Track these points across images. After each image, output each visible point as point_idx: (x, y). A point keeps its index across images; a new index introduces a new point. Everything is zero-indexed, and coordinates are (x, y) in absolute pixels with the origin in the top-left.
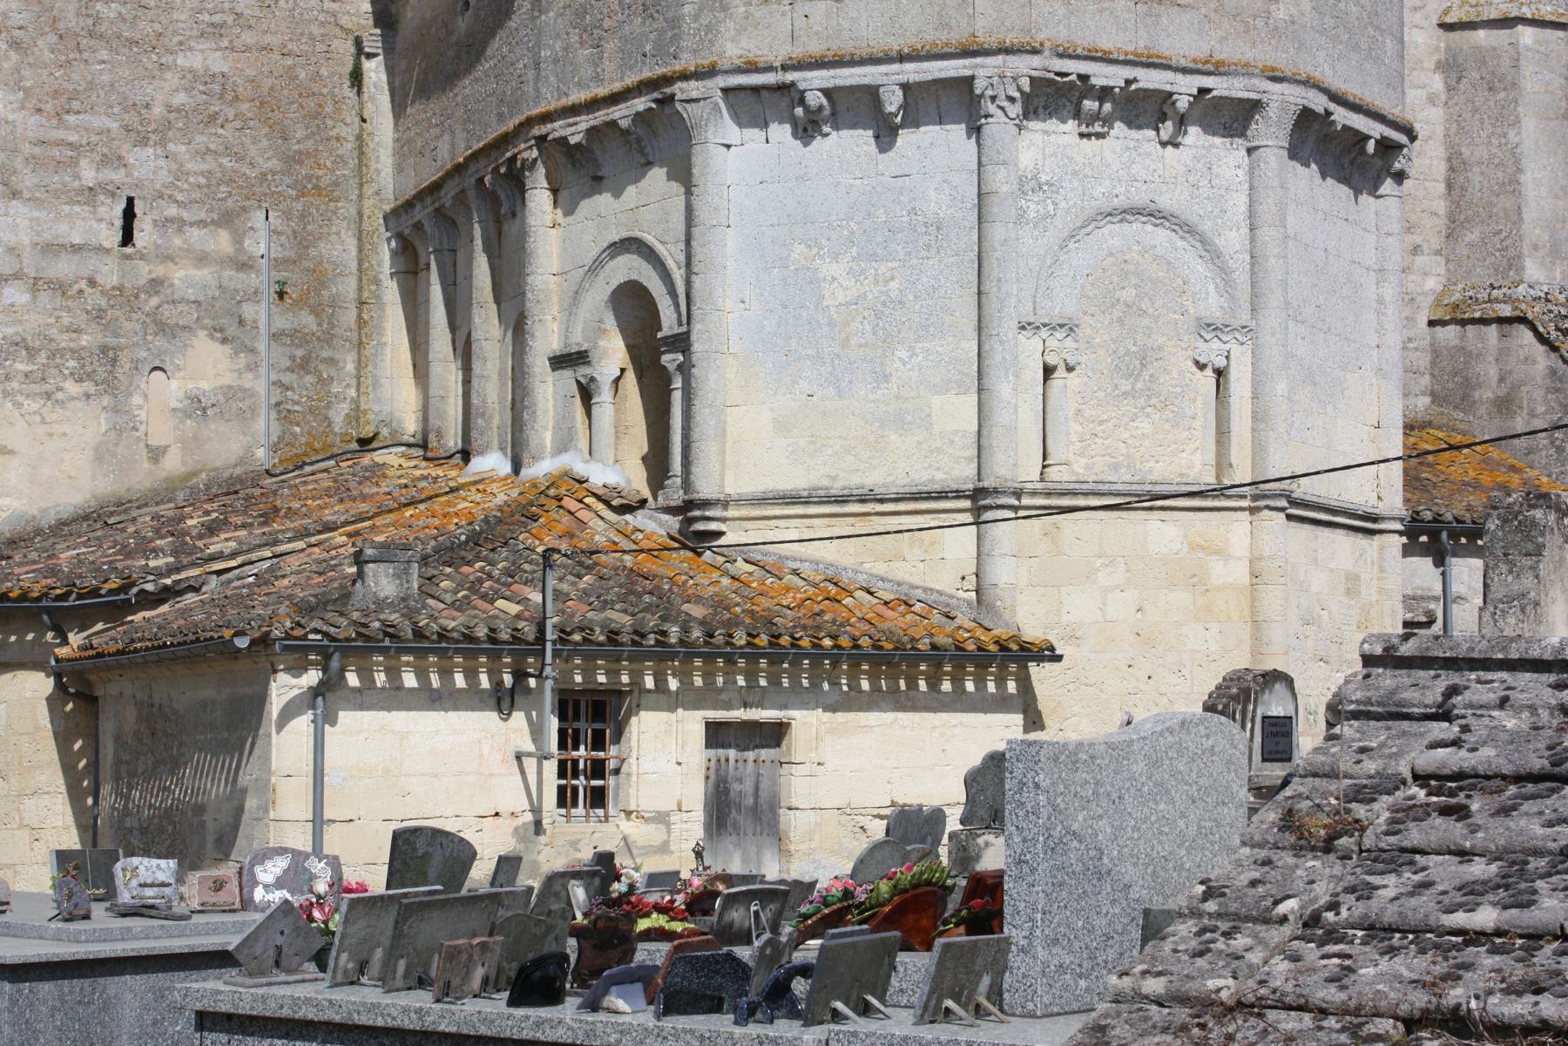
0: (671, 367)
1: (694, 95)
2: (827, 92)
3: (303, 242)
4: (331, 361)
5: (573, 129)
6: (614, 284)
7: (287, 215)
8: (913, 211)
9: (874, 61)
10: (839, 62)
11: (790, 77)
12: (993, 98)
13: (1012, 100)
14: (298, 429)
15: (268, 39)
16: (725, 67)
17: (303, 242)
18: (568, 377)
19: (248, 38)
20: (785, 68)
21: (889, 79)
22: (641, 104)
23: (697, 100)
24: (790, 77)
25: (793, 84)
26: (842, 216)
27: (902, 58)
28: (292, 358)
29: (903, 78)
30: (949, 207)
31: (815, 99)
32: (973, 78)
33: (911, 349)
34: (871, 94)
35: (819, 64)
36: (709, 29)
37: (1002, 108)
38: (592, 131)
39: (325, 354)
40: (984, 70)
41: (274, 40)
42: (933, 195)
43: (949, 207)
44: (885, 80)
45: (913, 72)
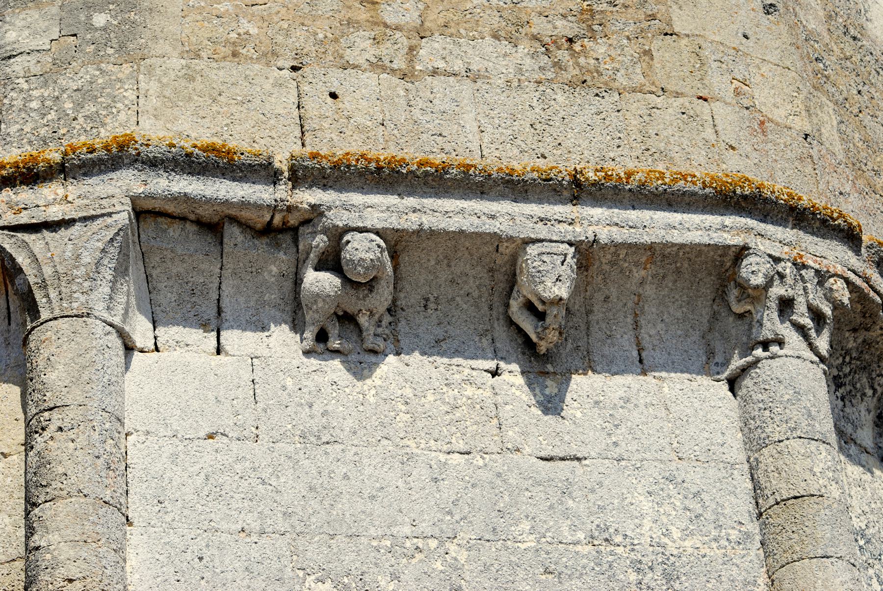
1: (55, 213)
8: (601, 537)
9: (514, 187)
10: (435, 180)
11: (307, 197)
12: (786, 305)
13: (817, 316)
16: (153, 152)
20: (300, 175)
21: (550, 240)
23: (67, 223)
24: (307, 197)
25: (317, 211)
26: (425, 527)
27: (578, 190)
29: (580, 232)
30: (687, 534)
31: (362, 249)
32: (742, 252)
34: (502, 263)
35: (385, 177)
36: (84, 95)
37: (801, 329)
40: (768, 244)
42: (646, 505)
43: (687, 534)
44: (542, 231)
45: (600, 222)
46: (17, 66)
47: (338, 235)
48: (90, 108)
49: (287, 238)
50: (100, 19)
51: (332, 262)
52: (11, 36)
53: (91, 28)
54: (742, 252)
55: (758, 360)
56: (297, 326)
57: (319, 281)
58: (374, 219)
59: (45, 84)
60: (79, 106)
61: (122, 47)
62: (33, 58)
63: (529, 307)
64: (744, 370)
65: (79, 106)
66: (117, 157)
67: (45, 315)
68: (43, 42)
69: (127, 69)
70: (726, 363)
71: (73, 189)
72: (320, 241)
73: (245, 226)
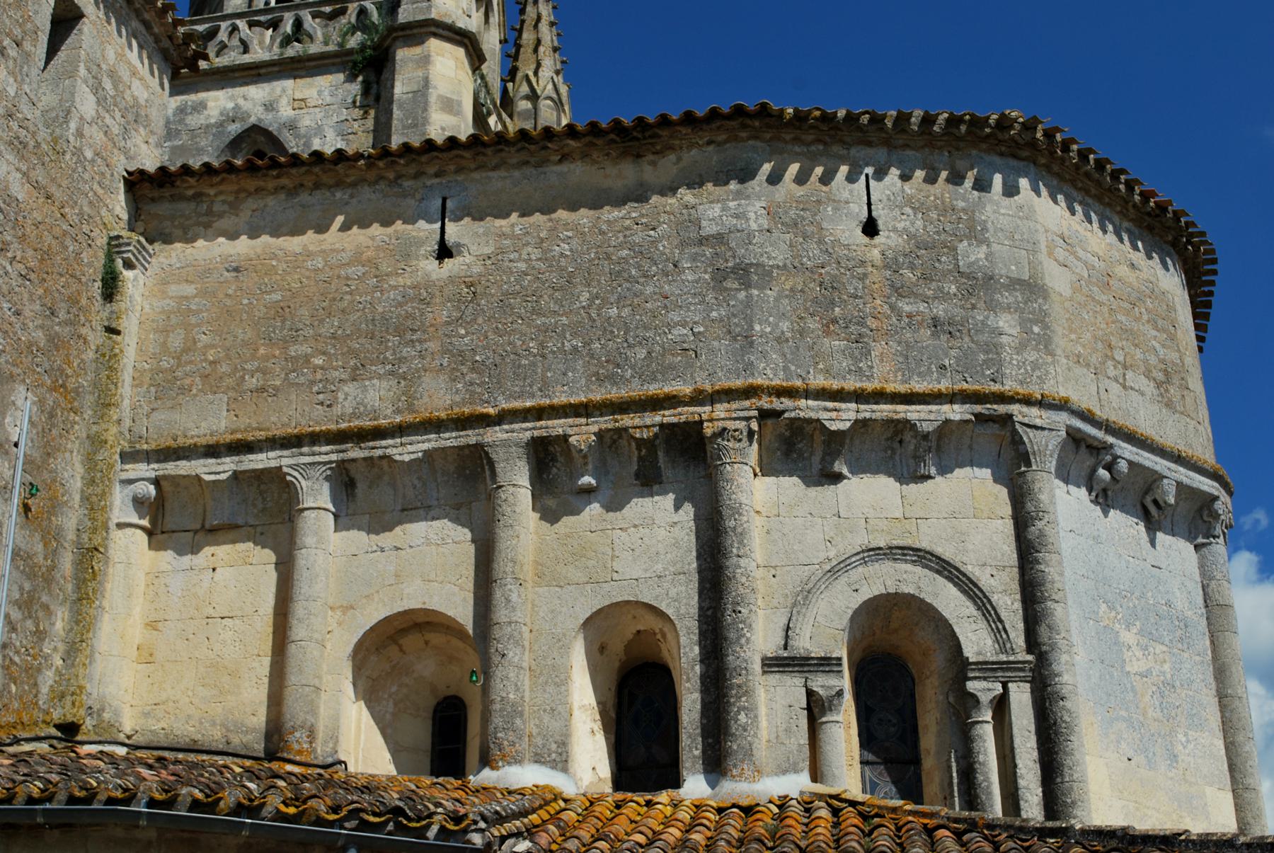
0: (985, 698)
1: (1038, 422)
2: (1130, 463)
3: (48, 448)
4: (46, 608)
5: (834, 415)
6: (867, 593)
7: (41, 402)
11: (1110, 439)
14: (13, 688)
15: (53, 189)
16: (1075, 407)
17: (48, 448)
18: (791, 689)
19: (39, 175)
22: (956, 412)
23: (1042, 429)
24: (1110, 439)
25: (1111, 446)
28: (21, 588)
31: (1123, 466)
32: (1217, 498)
33: (1186, 735)
38: (861, 425)
39: (45, 599)
41: (57, 194)
46: (1004, 339)
47: (1116, 457)
48: (1038, 373)
49: (1095, 452)
50: (1036, 329)
51: (1109, 467)
52: (1001, 324)
53: (1032, 332)
54: (1217, 498)
55: (1210, 543)
56: (1090, 491)
57: (1103, 473)
58: (1127, 455)
59: (1018, 354)
60: (1033, 370)
61: (1046, 347)
62: (1010, 339)
63: (1155, 502)
64: (1204, 545)
65: (1033, 370)
66: (1062, 405)
67: (1034, 467)
68: (1014, 332)
69: (1049, 359)
70: (1196, 538)
71: (1046, 414)
72: (1109, 458)
73: (1089, 447)
